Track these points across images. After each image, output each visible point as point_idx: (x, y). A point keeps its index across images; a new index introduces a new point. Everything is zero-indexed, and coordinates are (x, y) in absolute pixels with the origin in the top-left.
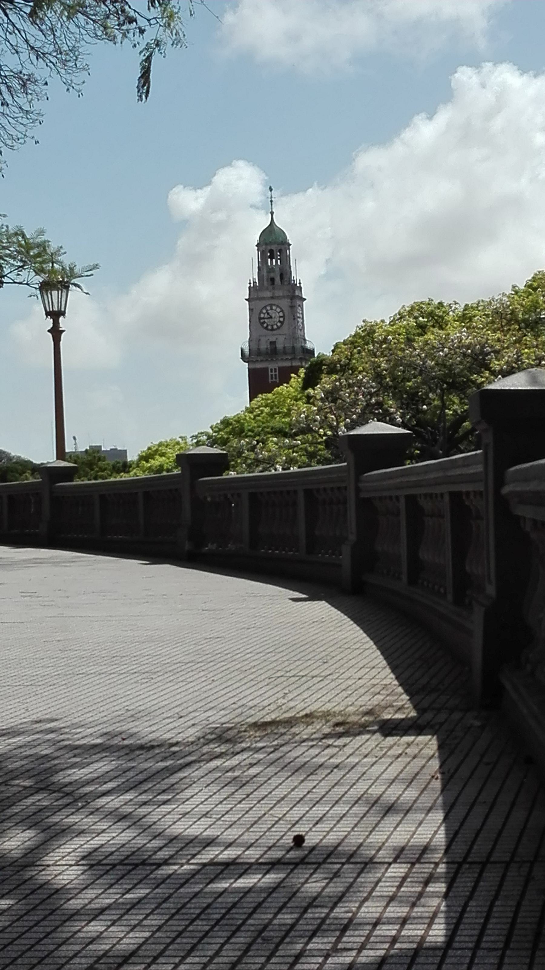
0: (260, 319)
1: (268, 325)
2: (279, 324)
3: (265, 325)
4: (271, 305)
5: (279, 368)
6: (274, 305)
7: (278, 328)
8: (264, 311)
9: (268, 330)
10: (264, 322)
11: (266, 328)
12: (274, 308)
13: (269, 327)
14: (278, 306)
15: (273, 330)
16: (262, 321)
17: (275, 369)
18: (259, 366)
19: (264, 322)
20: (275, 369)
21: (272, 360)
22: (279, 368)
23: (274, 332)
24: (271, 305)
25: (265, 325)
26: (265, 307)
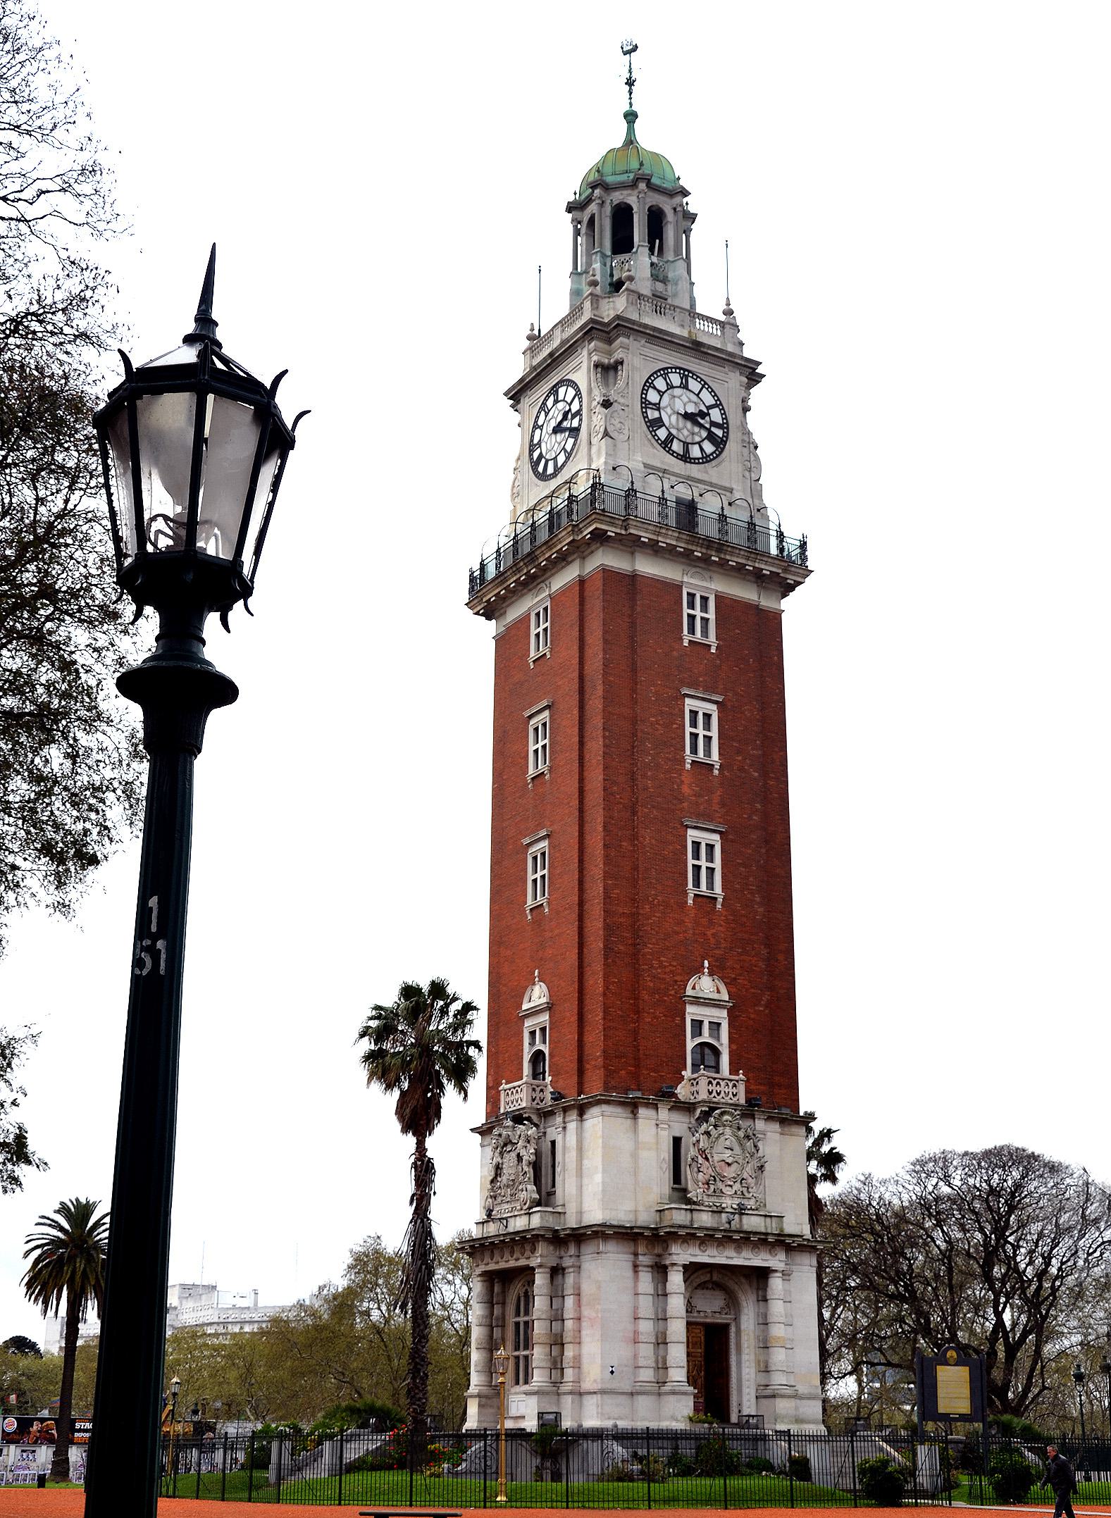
0: (645, 404)
1: (671, 437)
2: (709, 448)
3: (662, 434)
4: (685, 374)
5: (719, 598)
6: (697, 377)
7: (706, 459)
8: (660, 383)
9: (672, 453)
10: (658, 423)
11: (666, 444)
12: (694, 385)
13: (676, 446)
14: (705, 385)
15: (685, 458)
16: (652, 414)
17: (705, 600)
18: (647, 567)
19: (658, 423)
20: (705, 600)
21: (705, 560)
22: (719, 598)
23: (694, 471)
24: (685, 374)
25: (662, 434)
26: (664, 372)
